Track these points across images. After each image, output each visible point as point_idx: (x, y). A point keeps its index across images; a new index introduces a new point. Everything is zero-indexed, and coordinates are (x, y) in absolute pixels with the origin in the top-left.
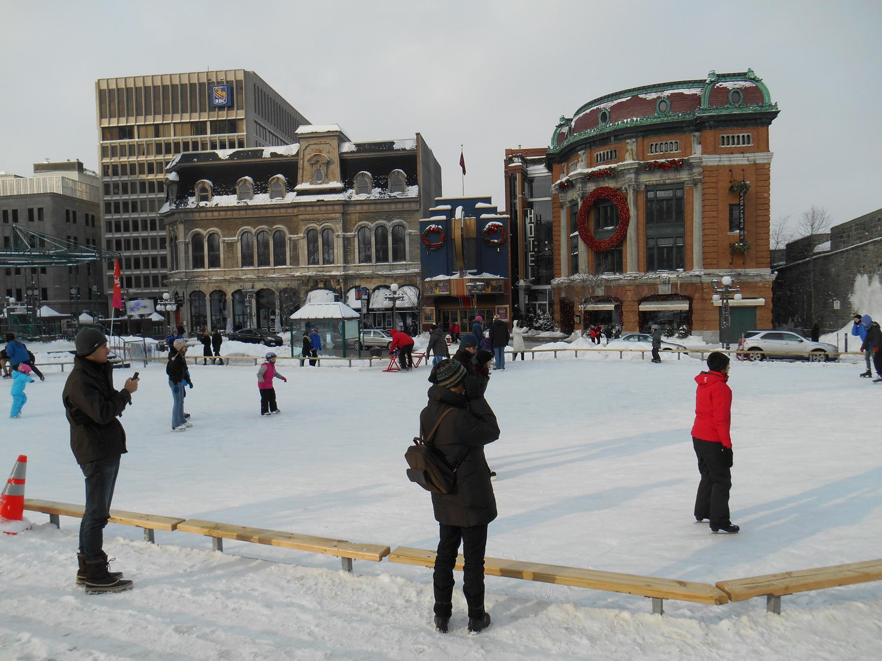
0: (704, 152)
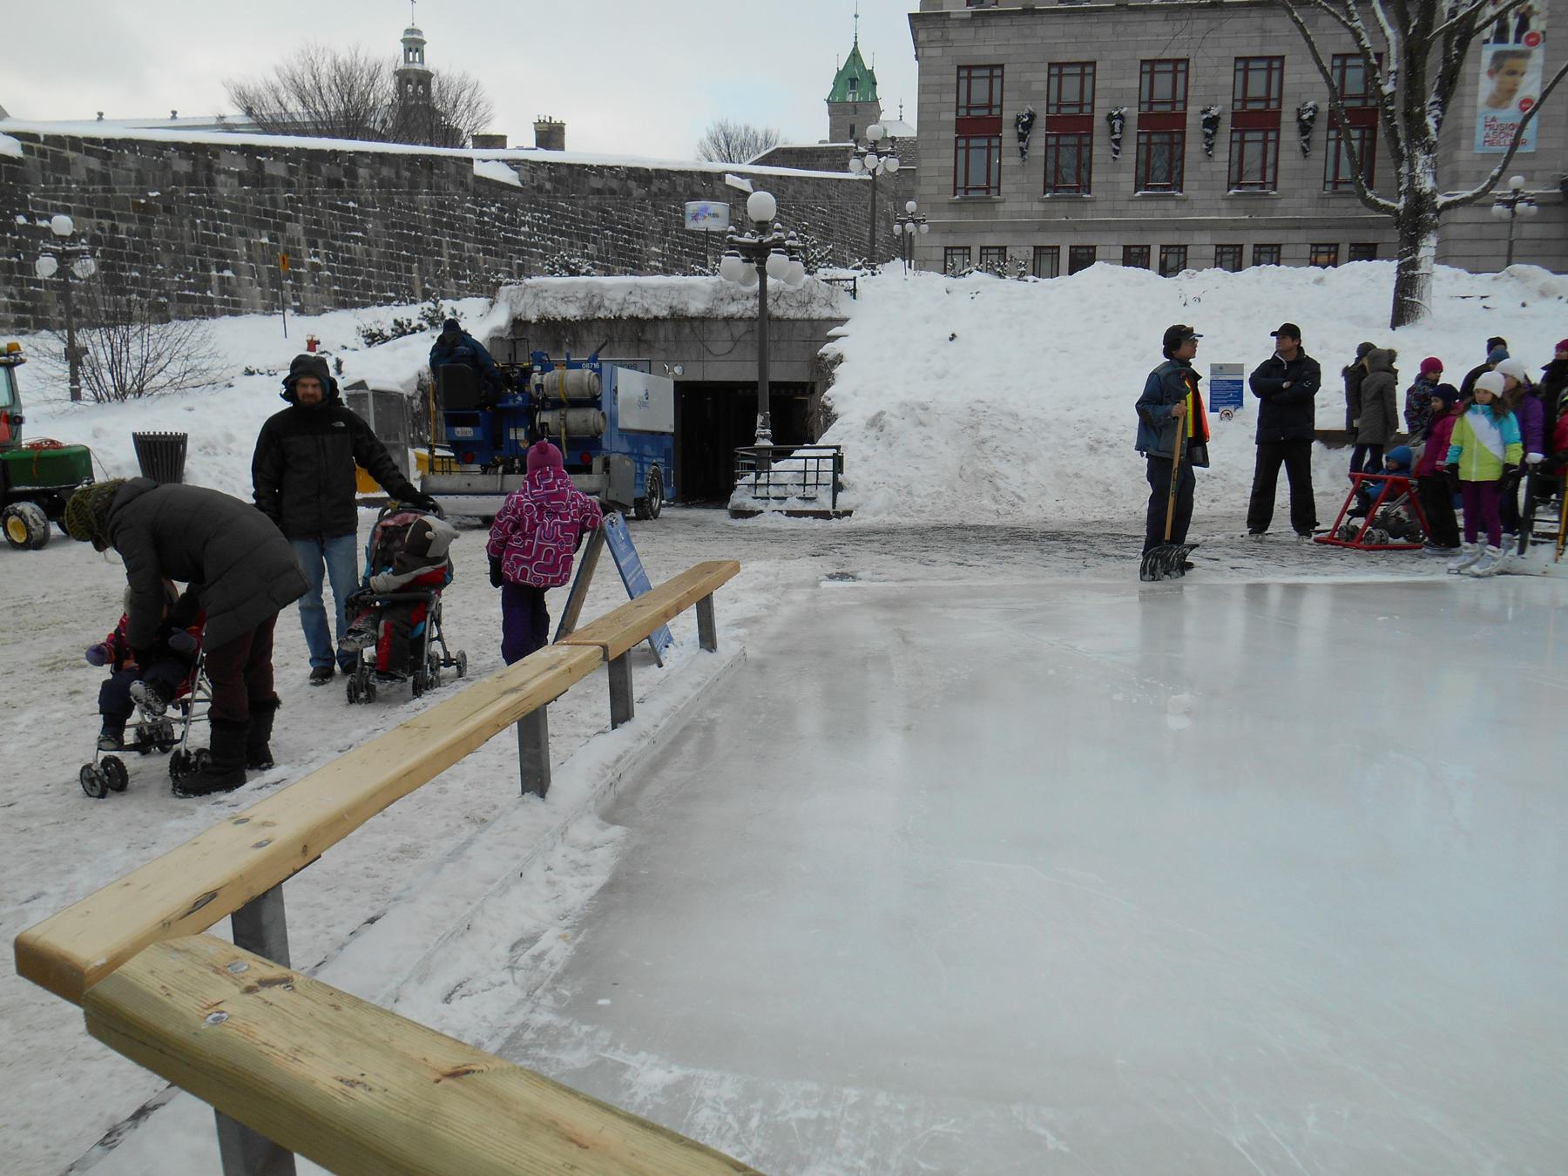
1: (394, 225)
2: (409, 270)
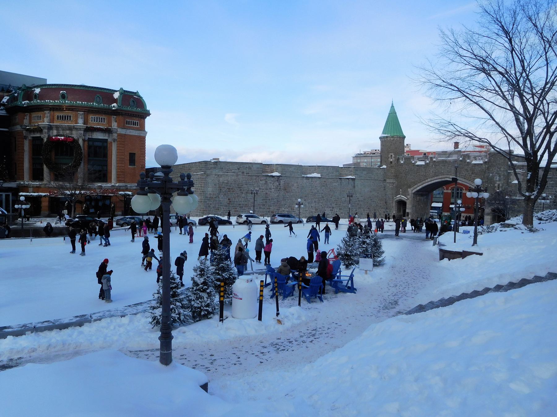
0: (119, 126)
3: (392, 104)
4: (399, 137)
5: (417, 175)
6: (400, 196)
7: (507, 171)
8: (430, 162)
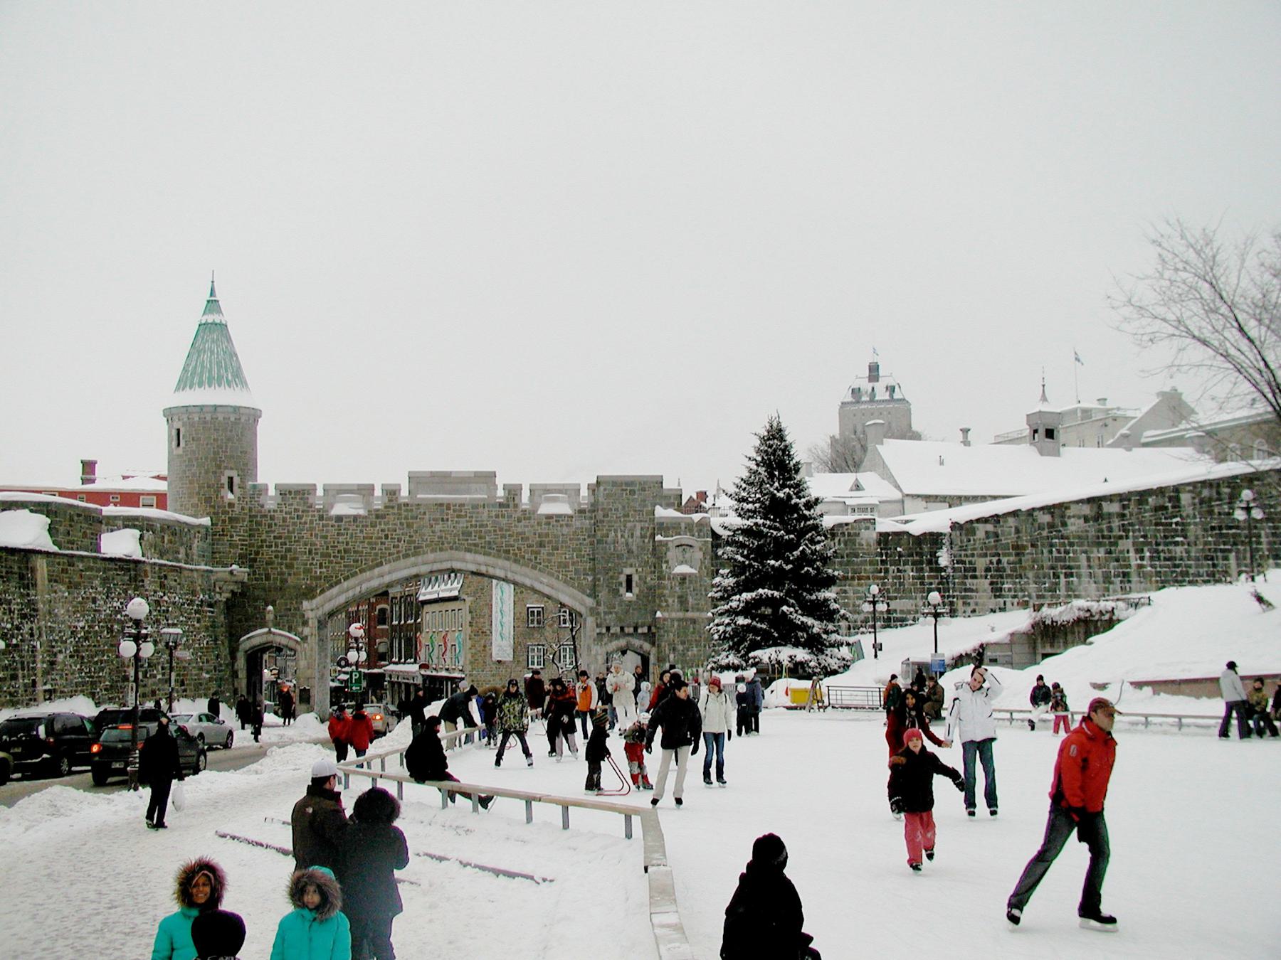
1: (1213, 528)
2: (1226, 558)
3: (212, 293)
4: (252, 412)
5: (339, 552)
6: (270, 632)
7: (653, 536)
8: (386, 507)
